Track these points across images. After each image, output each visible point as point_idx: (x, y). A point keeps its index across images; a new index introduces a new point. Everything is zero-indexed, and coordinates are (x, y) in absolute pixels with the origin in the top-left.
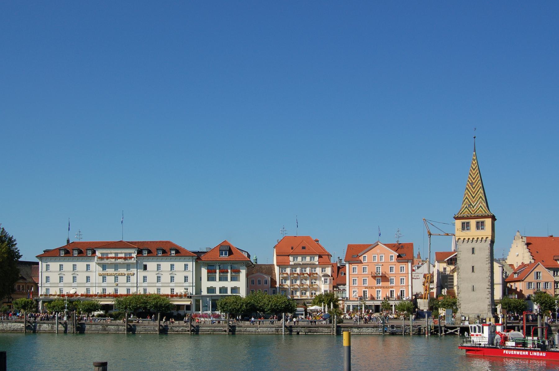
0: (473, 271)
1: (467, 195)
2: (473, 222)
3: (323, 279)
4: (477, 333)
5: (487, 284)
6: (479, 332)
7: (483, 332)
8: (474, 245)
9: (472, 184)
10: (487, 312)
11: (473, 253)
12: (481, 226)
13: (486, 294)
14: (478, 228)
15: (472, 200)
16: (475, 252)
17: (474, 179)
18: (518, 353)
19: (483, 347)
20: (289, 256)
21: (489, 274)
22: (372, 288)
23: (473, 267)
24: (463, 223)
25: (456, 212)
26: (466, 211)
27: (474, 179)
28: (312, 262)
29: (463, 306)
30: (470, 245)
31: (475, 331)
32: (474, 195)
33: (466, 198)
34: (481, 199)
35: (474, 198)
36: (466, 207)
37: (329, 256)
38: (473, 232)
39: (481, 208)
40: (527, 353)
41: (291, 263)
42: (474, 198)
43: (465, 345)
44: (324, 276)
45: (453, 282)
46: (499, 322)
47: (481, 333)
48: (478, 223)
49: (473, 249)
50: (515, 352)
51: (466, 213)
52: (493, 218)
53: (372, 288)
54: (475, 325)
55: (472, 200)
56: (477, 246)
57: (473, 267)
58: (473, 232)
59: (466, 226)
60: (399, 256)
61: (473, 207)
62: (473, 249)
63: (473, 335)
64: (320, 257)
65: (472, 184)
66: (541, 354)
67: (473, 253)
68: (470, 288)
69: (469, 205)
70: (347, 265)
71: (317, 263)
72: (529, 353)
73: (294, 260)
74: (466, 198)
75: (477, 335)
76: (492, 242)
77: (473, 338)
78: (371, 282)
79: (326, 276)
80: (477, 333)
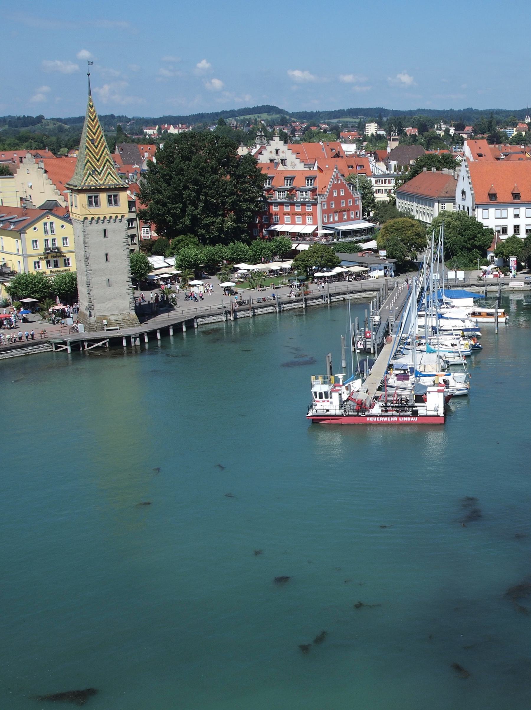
0: (107, 259)
1: (88, 157)
2: (103, 197)
4: (324, 399)
7: (331, 398)
8: (106, 226)
9: (93, 141)
10: (128, 311)
14: (110, 202)
15: (96, 164)
17: (95, 134)
23: (107, 255)
24: (90, 197)
26: (91, 180)
27: (95, 134)
30: (101, 227)
32: (98, 158)
33: (88, 161)
34: (108, 163)
35: (98, 161)
36: (90, 174)
38: (104, 208)
39: (110, 176)
40: (396, 419)
42: (98, 161)
46: (339, 382)
47: (329, 399)
48: (110, 196)
49: (105, 231)
50: (381, 419)
55: (96, 164)
56: (109, 227)
57: (107, 255)
58: (104, 208)
59: (93, 202)
61: (100, 174)
62: (105, 231)
63: (318, 401)
65: (93, 141)
67: (105, 235)
68: (105, 283)
69: (92, 171)
72: (398, 419)
74: (88, 161)
75: (324, 401)
80: (324, 399)
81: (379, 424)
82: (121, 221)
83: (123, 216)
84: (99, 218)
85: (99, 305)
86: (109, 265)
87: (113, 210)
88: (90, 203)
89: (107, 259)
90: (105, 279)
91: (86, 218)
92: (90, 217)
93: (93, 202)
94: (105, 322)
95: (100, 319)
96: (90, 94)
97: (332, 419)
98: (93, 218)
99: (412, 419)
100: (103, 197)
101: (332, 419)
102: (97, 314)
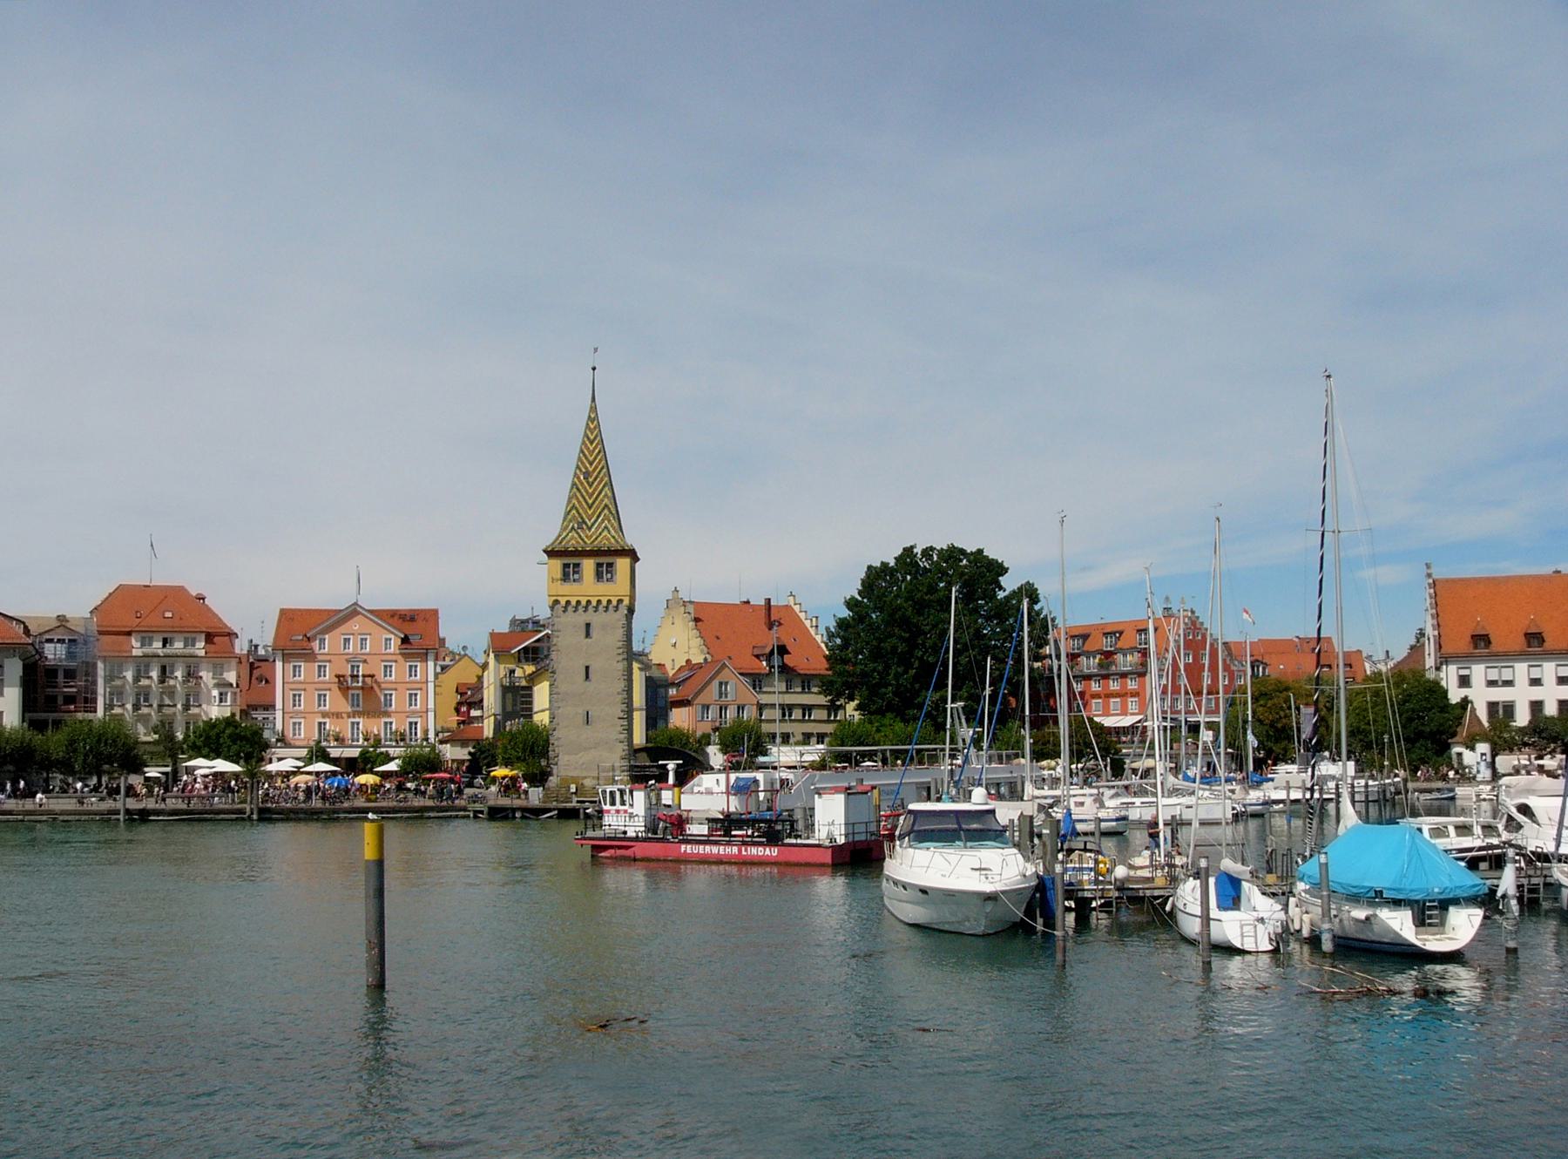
0: (587, 677)
2: (588, 565)
3: (215, 693)
4: (618, 806)
5: (618, 710)
6: (623, 803)
8: (590, 616)
9: (587, 475)
11: (588, 635)
12: (604, 572)
13: (615, 732)
14: (599, 576)
16: (594, 632)
18: (715, 849)
19: (631, 839)
20: (129, 634)
21: (622, 685)
22: (338, 715)
23: (587, 668)
24: (566, 566)
25: (548, 540)
28: (189, 651)
29: (563, 759)
30: (582, 618)
31: (613, 803)
37: (231, 635)
40: (735, 850)
41: (135, 652)
43: (590, 833)
44: (217, 685)
45: (531, 703)
48: (599, 565)
49: (588, 625)
50: (708, 848)
51: (573, 542)
52: (632, 555)
53: (338, 715)
54: (615, 788)
56: (597, 619)
57: (587, 668)
59: (569, 574)
60: (405, 640)
62: (588, 625)
64: (209, 638)
66: (768, 852)
67: (588, 635)
68: (582, 718)
70: (279, 665)
71: (202, 653)
73: (143, 645)
74: (574, 507)
75: (618, 811)
76: (631, 610)
77: (607, 820)
78: (335, 701)
79: (223, 685)
80: (618, 806)
81: (705, 861)
82: (617, 608)
83: (620, 601)
84: (578, 602)
85: (566, 758)
86: (590, 686)
87: (606, 591)
88: (565, 577)
89: (587, 677)
90: (581, 711)
91: (557, 602)
92: (563, 601)
93: (569, 574)
94: (573, 788)
95: (565, 783)
96: (593, 399)
97: (620, 847)
98: (568, 603)
99: (768, 852)
100: (588, 565)
101: (620, 847)
102: (563, 773)
